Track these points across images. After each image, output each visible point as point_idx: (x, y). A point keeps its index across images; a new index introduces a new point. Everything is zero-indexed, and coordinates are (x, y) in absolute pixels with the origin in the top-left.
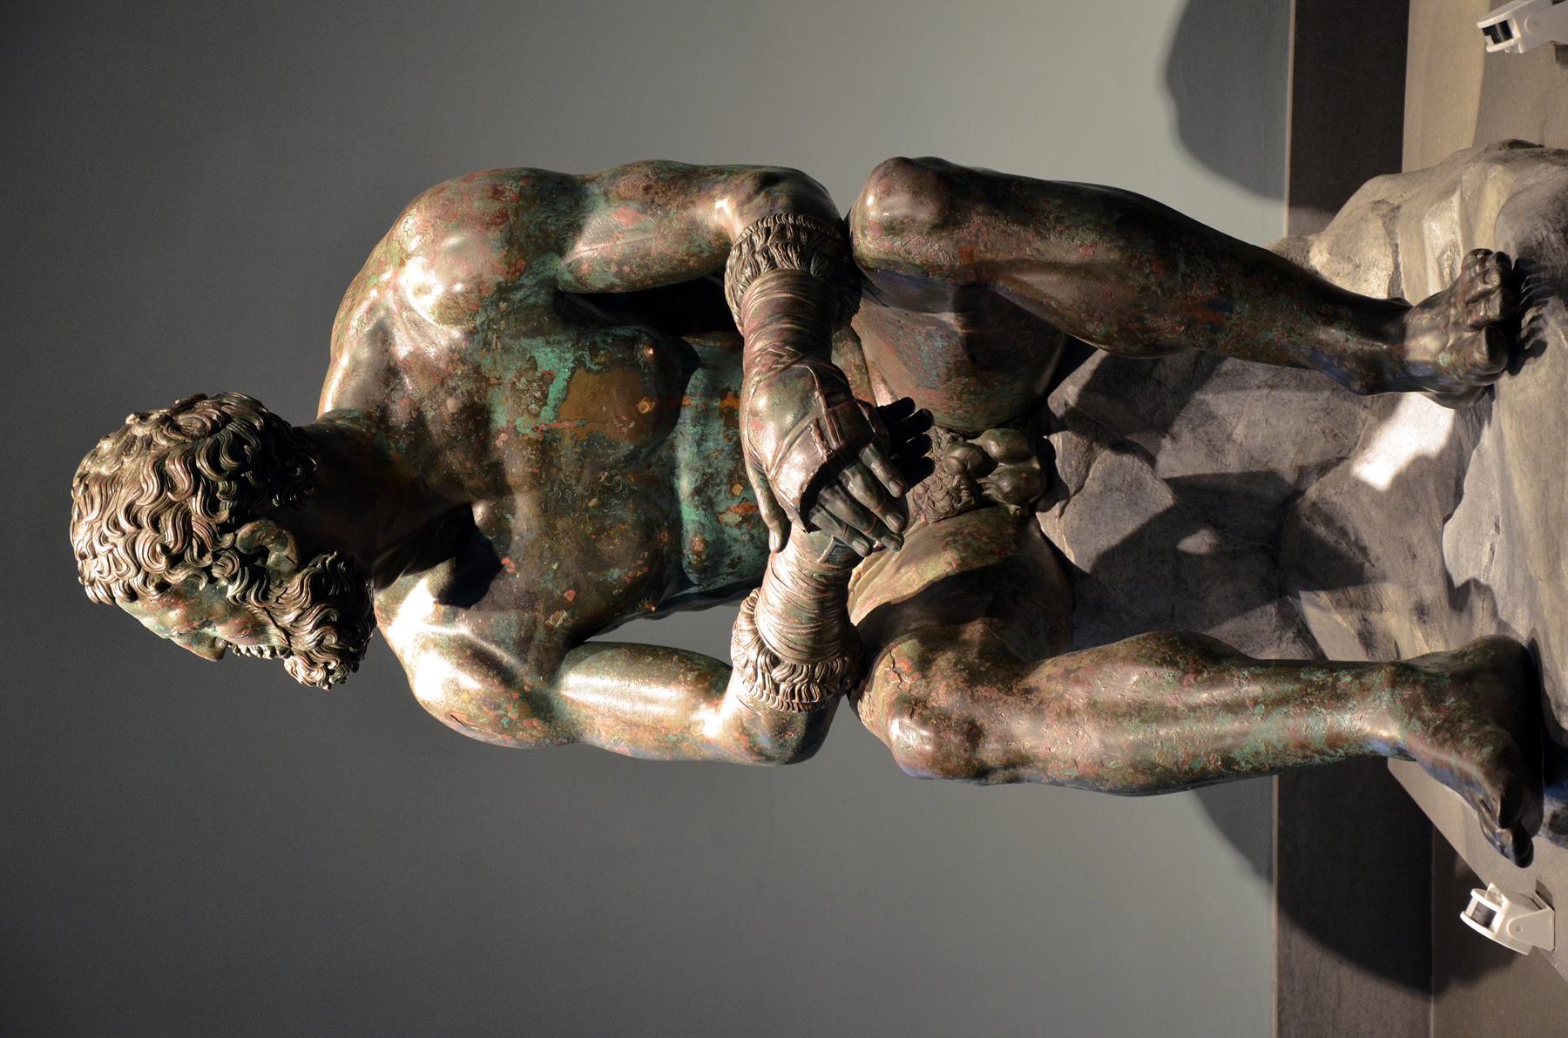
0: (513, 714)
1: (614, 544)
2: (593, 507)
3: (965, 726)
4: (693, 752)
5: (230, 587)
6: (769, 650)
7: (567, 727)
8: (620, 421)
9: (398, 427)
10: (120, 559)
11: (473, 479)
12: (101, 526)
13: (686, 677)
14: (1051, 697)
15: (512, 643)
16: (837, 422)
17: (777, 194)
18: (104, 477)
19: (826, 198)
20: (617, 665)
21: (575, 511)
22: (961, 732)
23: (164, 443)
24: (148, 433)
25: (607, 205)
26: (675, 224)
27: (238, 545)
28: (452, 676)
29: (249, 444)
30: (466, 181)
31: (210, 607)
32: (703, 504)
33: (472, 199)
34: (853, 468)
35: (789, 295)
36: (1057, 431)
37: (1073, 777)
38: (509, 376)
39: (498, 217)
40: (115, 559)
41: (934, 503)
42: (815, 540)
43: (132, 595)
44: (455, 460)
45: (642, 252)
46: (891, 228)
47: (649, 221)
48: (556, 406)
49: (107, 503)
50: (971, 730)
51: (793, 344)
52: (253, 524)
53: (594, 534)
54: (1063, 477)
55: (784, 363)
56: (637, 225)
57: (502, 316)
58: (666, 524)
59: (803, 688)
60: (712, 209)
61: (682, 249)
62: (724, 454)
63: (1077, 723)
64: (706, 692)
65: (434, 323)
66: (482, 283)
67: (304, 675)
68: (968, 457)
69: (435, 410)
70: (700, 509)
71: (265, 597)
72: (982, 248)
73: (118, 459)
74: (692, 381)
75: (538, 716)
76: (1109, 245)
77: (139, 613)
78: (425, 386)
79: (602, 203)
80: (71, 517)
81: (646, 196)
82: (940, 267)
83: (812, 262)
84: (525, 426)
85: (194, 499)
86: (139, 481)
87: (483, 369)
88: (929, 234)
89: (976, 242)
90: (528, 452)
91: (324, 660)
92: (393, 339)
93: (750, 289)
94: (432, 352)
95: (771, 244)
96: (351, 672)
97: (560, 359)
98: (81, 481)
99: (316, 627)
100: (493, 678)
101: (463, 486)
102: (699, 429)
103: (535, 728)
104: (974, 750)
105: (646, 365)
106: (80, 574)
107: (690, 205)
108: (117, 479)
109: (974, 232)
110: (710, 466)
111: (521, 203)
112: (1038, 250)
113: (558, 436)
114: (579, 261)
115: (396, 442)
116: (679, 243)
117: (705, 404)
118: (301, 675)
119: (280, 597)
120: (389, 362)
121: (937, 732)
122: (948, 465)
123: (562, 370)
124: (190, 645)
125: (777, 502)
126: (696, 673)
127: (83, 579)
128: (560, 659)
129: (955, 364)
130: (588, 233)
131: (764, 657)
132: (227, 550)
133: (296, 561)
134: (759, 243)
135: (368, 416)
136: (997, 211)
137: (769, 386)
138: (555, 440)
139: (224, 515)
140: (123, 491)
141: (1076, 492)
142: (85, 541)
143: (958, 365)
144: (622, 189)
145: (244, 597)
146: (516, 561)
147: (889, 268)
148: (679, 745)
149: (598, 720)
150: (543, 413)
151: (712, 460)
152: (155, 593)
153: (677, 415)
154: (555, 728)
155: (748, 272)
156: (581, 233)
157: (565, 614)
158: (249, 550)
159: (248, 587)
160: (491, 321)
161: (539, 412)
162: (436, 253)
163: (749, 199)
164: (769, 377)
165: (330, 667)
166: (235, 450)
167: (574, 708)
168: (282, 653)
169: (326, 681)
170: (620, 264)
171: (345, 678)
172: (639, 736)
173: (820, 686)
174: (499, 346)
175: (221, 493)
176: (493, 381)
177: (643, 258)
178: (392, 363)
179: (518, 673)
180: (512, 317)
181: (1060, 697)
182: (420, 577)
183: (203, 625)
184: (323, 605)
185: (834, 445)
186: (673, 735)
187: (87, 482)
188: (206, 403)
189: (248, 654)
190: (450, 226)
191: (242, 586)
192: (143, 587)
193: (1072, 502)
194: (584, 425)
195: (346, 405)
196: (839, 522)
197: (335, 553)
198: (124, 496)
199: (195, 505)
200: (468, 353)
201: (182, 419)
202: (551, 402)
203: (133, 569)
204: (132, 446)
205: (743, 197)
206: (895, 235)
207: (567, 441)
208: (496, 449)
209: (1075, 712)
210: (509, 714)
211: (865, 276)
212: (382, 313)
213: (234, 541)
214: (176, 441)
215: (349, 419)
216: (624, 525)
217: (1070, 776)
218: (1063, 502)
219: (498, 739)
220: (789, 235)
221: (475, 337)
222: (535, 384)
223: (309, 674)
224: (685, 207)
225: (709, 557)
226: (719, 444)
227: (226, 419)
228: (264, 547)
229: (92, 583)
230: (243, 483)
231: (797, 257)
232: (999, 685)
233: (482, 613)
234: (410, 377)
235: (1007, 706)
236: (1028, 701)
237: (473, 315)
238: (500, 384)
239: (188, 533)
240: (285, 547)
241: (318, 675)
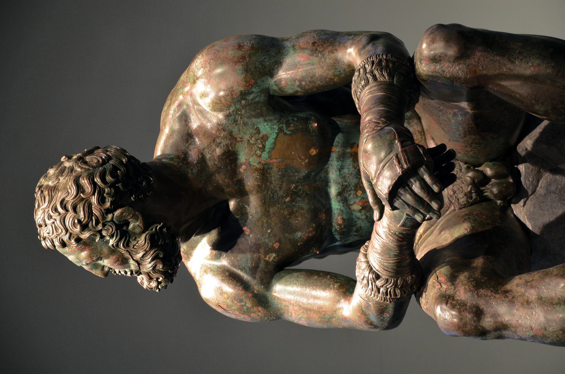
0: (249, 304)
1: (298, 220)
2: (288, 201)
3: (474, 309)
4: (338, 324)
5: (111, 240)
6: (375, 271)
7: (276, 311)
8: (301, 159)
9: (193, 162)
10: (58, 227)
11: (229, 188)
12: (49, 211)
13: (334, 286)
14: (518, 294)
15: (248, 269)
16: (407, 155)
17: (378, 44)
18: (50, 187)
19: (403, 46)
20: (300, 280)
21: (279, 204)
22: (472, 312)
23: (79, 170)
24: (72, 165)
25: (294, 52)
26: (328, 60)
27: (114, 220)
28: (219, 286)
29: (120, 170)
30: (225, 41)
31: (102, 250)
32: (342, 200)
33: (228, 50)
34: (415, 178)
35: (383, 94)
36: (522, 163)
37: (530, 336)
38: (247, 137)
39: (241, 59)
40: (55, 227)
41: (458, 200)
42: (397, 215)
43: (64, 245)
44: (220, 179)
45: (311, 75)
46: (435, 59)
47: (315, 60)
48: (269, 152)
49: (52, 199)
50: (477, 311)
51: (385, 117)
52: (122, 209)
53: (289, 215)
54: (525, 187)
55: (380, 127)
56: (308, 61)
57: (243, 108)
58: (324, 210)
59: (392, 290)
60: (346, 52)
61: (331, 73)
62: (353, 175)
63: (532, 308)
64: (344, 293)
65: (210, 111)
66: (233, 91)
67: (147, 284)
68: (476, 176)
69: (210, 154)
70: (341, 203)
71: (128, 245)
72: (481, 68)
73: (57, 178)
74: (337, 139)
75: (262, 306)
76: (546, 65)
77: (67, 253)
78: (206, 142)
79: (291, 51)
80: (34, 207)
81: (313, 47)
82: (460, 78)
83: (395, 77)
84: (254, 162)
85: (93, 197)
86: (67, 188)
87: (234, 134)
88: (454, 62)
89: (478, 66)
90: (256, 175)
91: (156, 277)
92: (190, 119)
93: (364, 91)
94: (209, 125)
95: (374, 69)
96: (170, 283)
97: (272, 129)
98: (39, 189)
99: (152, 260)
100: (239, 287)
101: (224, 192)
102: (340, 163)
103: (260, 311)
104: (479, 322)
105: (313, 131)
106: (39, 234)
107: (335, 51)
108: (56, 187)
109: (477, 60)
110: (345, 182)
111: (252, 52)
112: (510, 69)
113: (270, 166)
114: (280, 80)
115: (192, 170)
116: (329, 70)
117: (343, 151)
118: (145, 285)
119: (135, 245)
120: (188, 131)
121: (460, 312)
122: (466, 180)
123: (272, 134)
124: (92, 269)
125: (377, 196)
126: (339, 284)
127: (40, 237)
128: (272, 277)
129: (469, 128)
130: (285, 66)
131: (372, 275)
132: (109, 222)
133: (142, 228)
134: (368, 68)
135: (178, 157)
136: (489, 50)
137: (373, 138)
138: (269, 168)
139: (108, 204)
140: (59, 193)
141: (532, 194)
142: (41, 218)
143: (470, 129)
144: (301, 44)
145: (117, 245)
146: (250, 228)
147: (433, 79)
148: (331, 320)
149: (291, 307)
150: (263, 155)
151: (347, 178)
152: (74, 243)
153: (329, 156)
154: (270, 312)
155: (363, 83)
156: (281, 66)
157: (274, 255)
158: (120, 222)
159: (119, 240)
160: (237, 110)
161: (261, 155)
162: (211, 77)
163: (364, 47)
164: (373, 134)
165: (159, 280)
166: (113, 173)
167: (279, 301)
168: (136, 273)
169: (157, 287)
170: (300, 81)
171: (166, 286)
172: (311, 315)
173: (401, 289)
174: (242, 122)
175: (106, 194)
176: (239, 139)
177: (311, 78)
178: (190, 131)
179: (251, 284)
180: (248, 108)
181: (523, 295)
182: (203, 237)
183: (98, 259)
184: (156, 249)
185: (405, 166)
186: (328, 315)
187: (42, 189)
188: (100, 150)
189: (120, 274)
190: (217, 63)
191: (117, 239)
192: (69, 241)
193: (530, 199)
194: (283, 161)
195: (167, 152)
196: (408, 205)
197: (162, 224)
198: (60, 196)
199: (94, 200)
200: (226, 126)
201: (88, 158)
202: (267, 149)
203: (64, 232)
204: (64, 172)
205: (361, 46)
206: (437, 63)
207: (275, 169)
208: (240, 173)
209: (531, 302)
210: (247, 305)
211: (421, 83)
212: (185, 107)
213: (113, 218)
214: (85, 169)
215: (169, 159)
216: (303, 211)
217: (529, 335)
218: (525, 199)
219: (242, 317)
220: (383, 64)
221: (230, 118)
222: (259, 141)
223: (149, 284)
224: (332, 52)
225: (345, 227)
226: (350, 171)
227: (109, 158)
228: (127, 220)
229: (44, 239)
230: (117, 189)
231: (388, 75)
232: (492, 289)
233: (233, 254)
234: (198, 138)
235: (495, 299)
236: (506, 297)
237: (229, 107)
238: (242, 141)
239: (90, 214)
240: (137, 221)
241: (154, 284)
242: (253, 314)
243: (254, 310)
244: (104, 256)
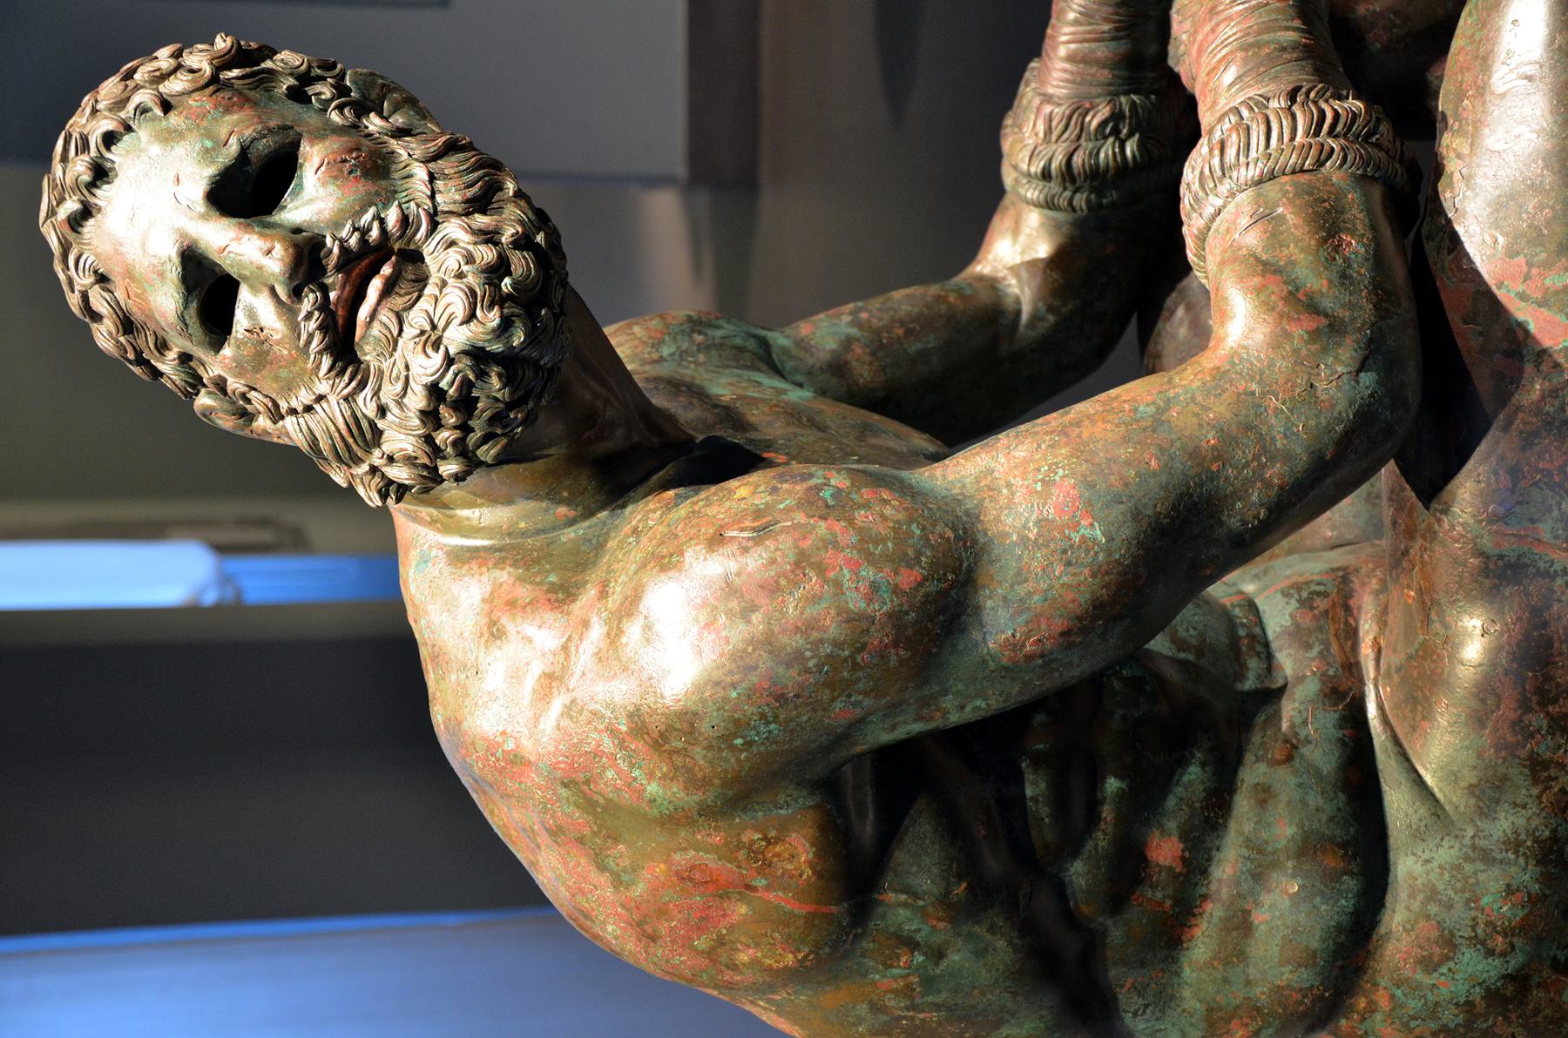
103: (886, 502)
165: (505, 239)
172: (1085, 435)
180: (713, 352)
186: (1148, 405)
210: (833, 482)
242: (862, 512)
243: (861, 496)
244: (309, 132)
